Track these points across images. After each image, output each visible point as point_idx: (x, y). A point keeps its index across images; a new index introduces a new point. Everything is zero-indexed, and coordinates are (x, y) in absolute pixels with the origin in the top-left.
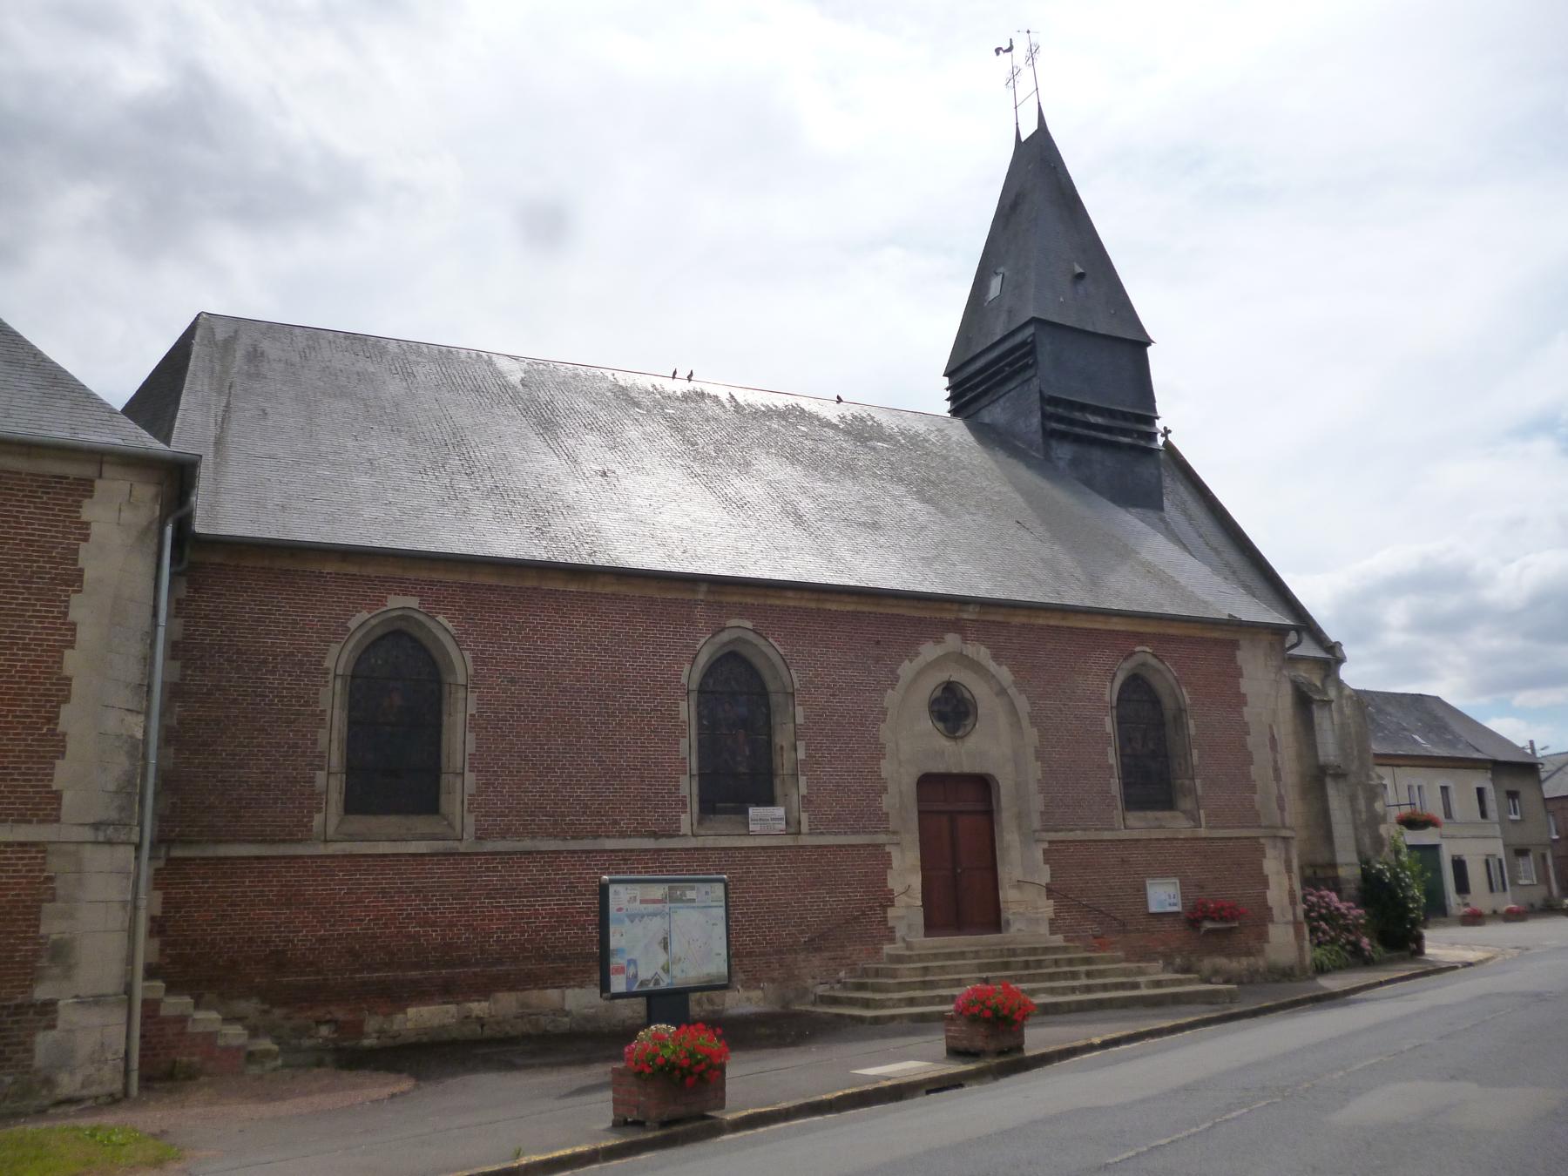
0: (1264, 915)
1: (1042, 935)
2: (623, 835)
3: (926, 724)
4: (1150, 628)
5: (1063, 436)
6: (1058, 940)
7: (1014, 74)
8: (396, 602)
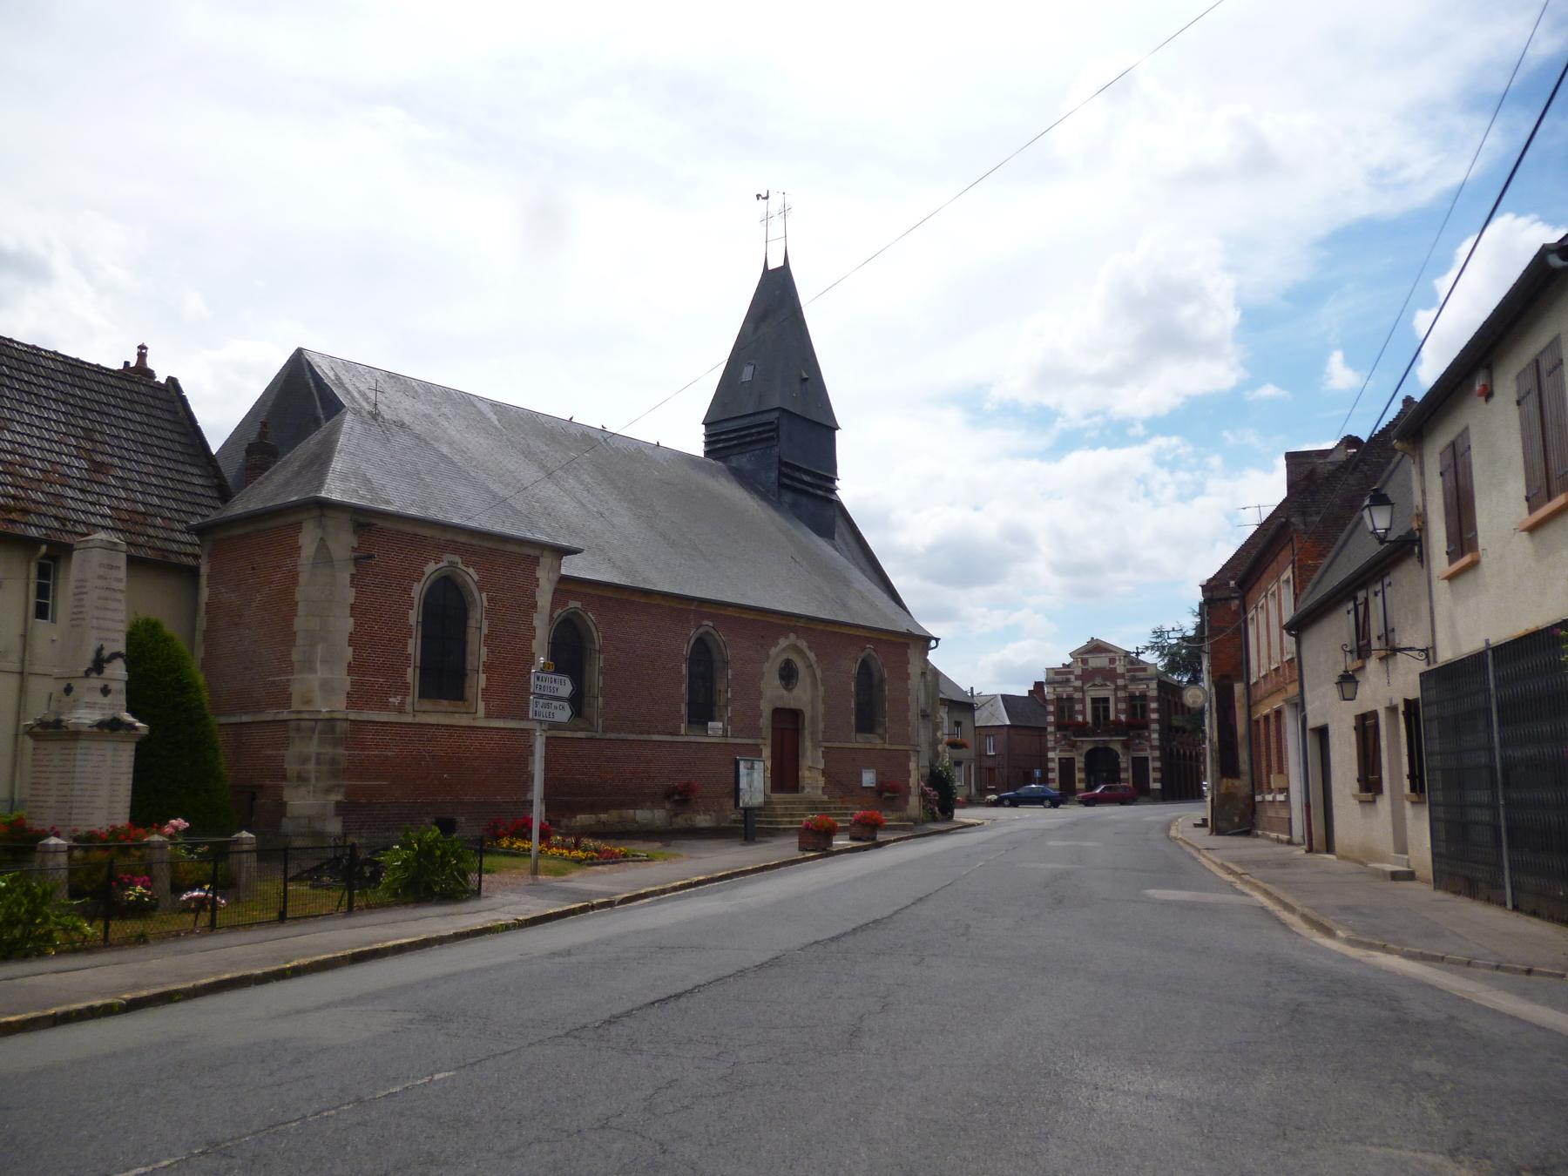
0: (906, 791)
1: (819, 795)
2: (659, 733)
3: (777, 682)
4: (874, 635)
5: (788, 487)
6: (825, 798)
7: (767, 218)
8: (431, 567)
